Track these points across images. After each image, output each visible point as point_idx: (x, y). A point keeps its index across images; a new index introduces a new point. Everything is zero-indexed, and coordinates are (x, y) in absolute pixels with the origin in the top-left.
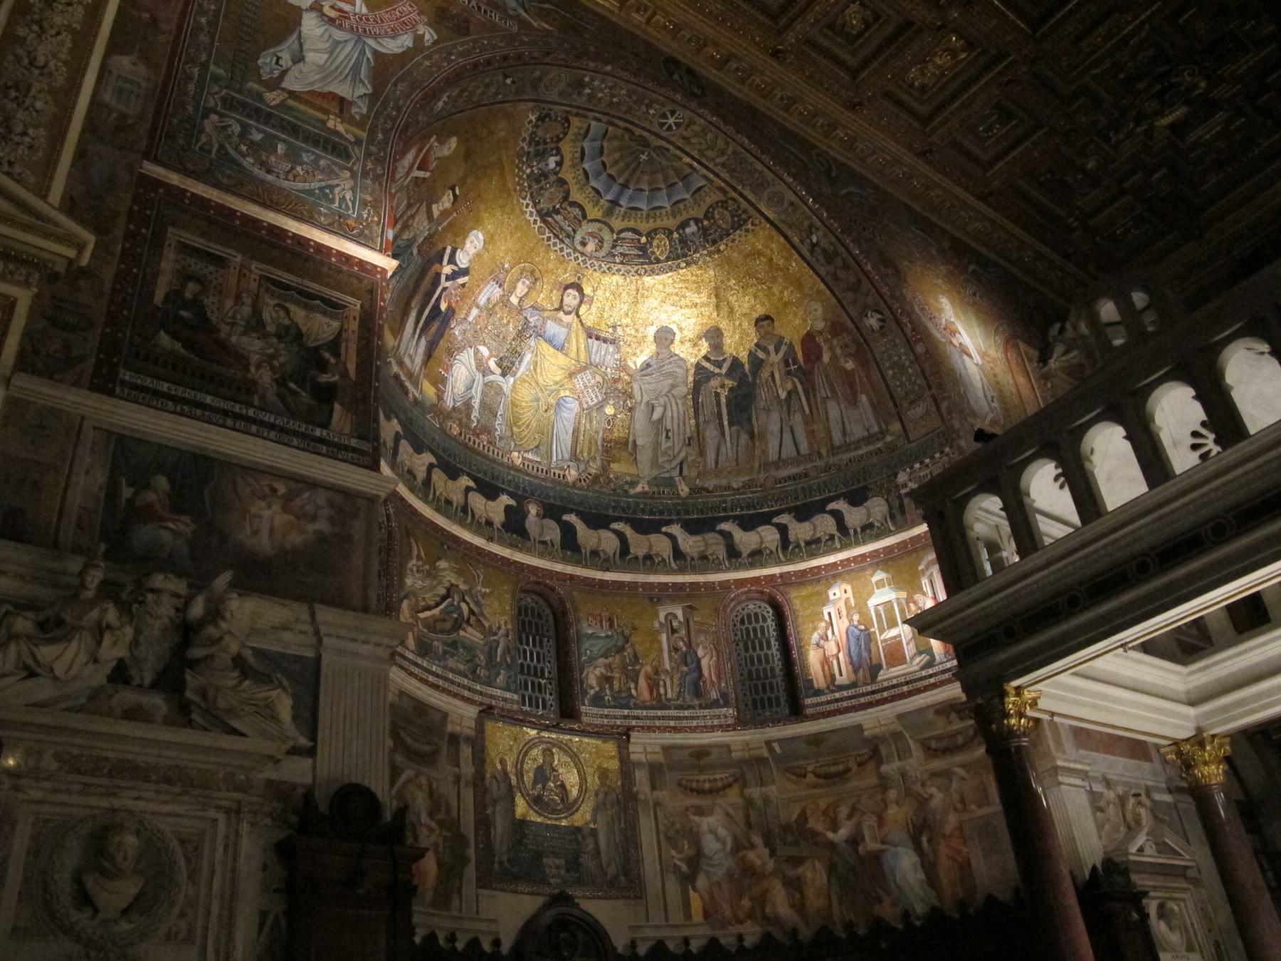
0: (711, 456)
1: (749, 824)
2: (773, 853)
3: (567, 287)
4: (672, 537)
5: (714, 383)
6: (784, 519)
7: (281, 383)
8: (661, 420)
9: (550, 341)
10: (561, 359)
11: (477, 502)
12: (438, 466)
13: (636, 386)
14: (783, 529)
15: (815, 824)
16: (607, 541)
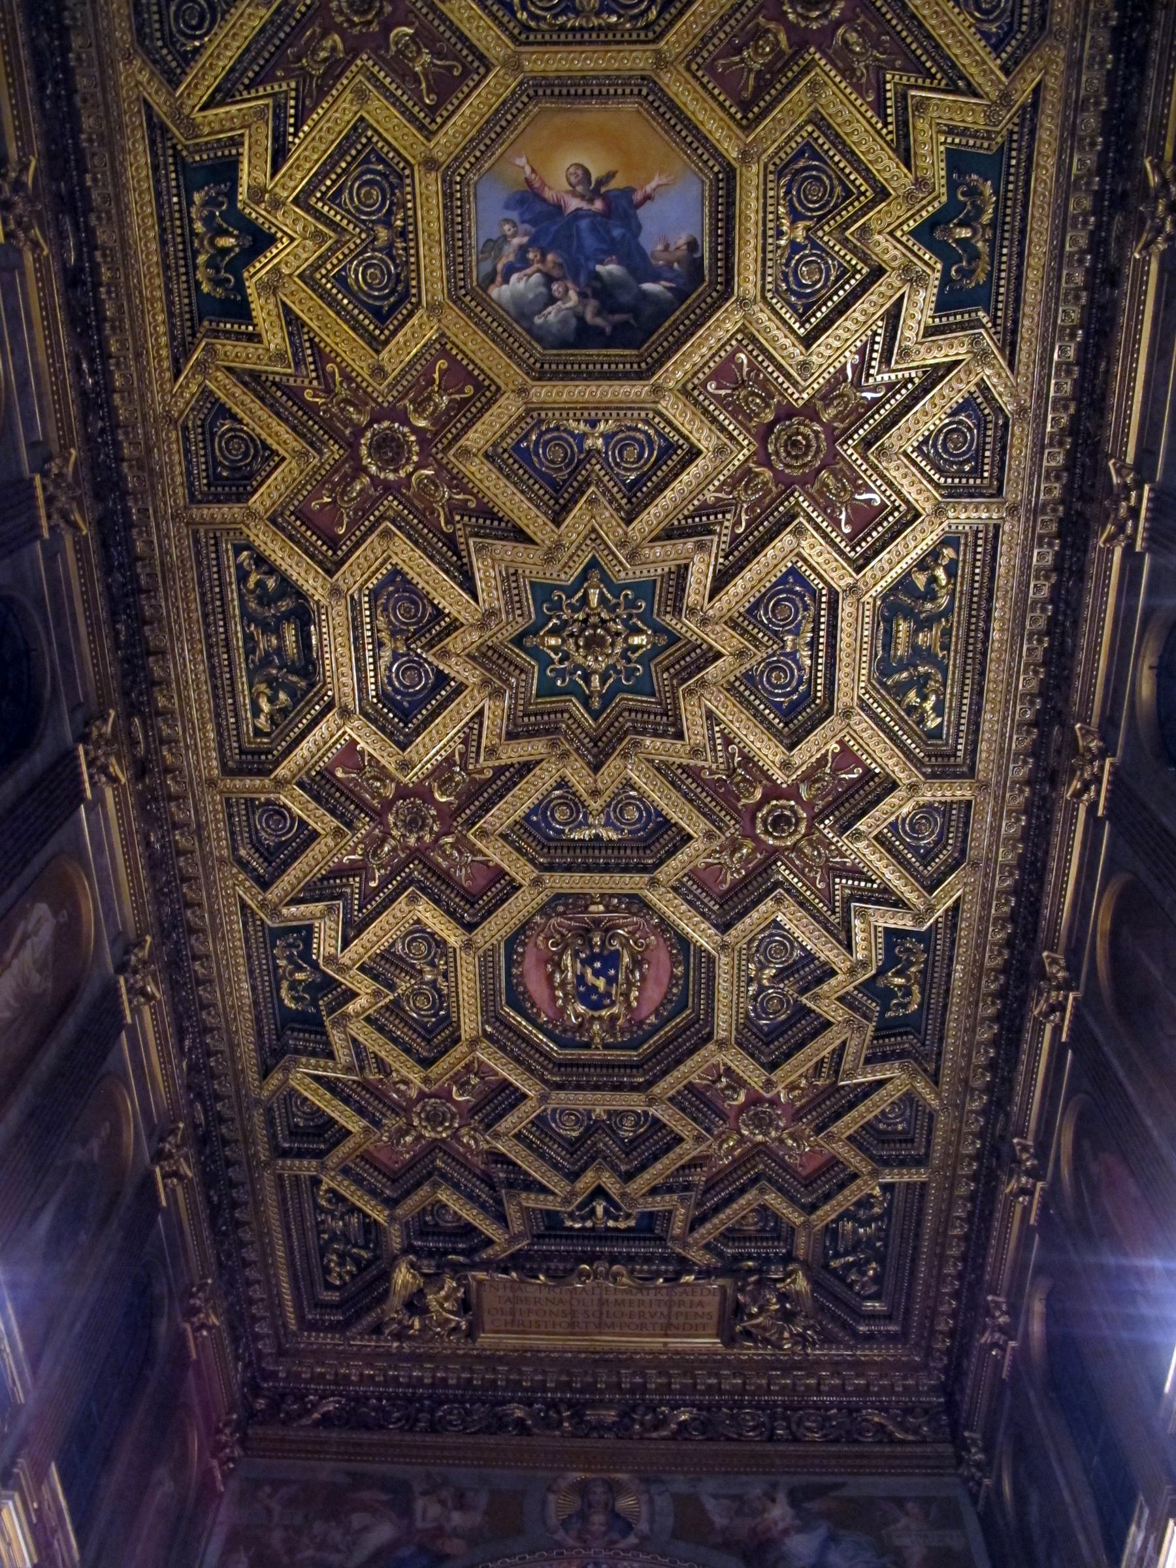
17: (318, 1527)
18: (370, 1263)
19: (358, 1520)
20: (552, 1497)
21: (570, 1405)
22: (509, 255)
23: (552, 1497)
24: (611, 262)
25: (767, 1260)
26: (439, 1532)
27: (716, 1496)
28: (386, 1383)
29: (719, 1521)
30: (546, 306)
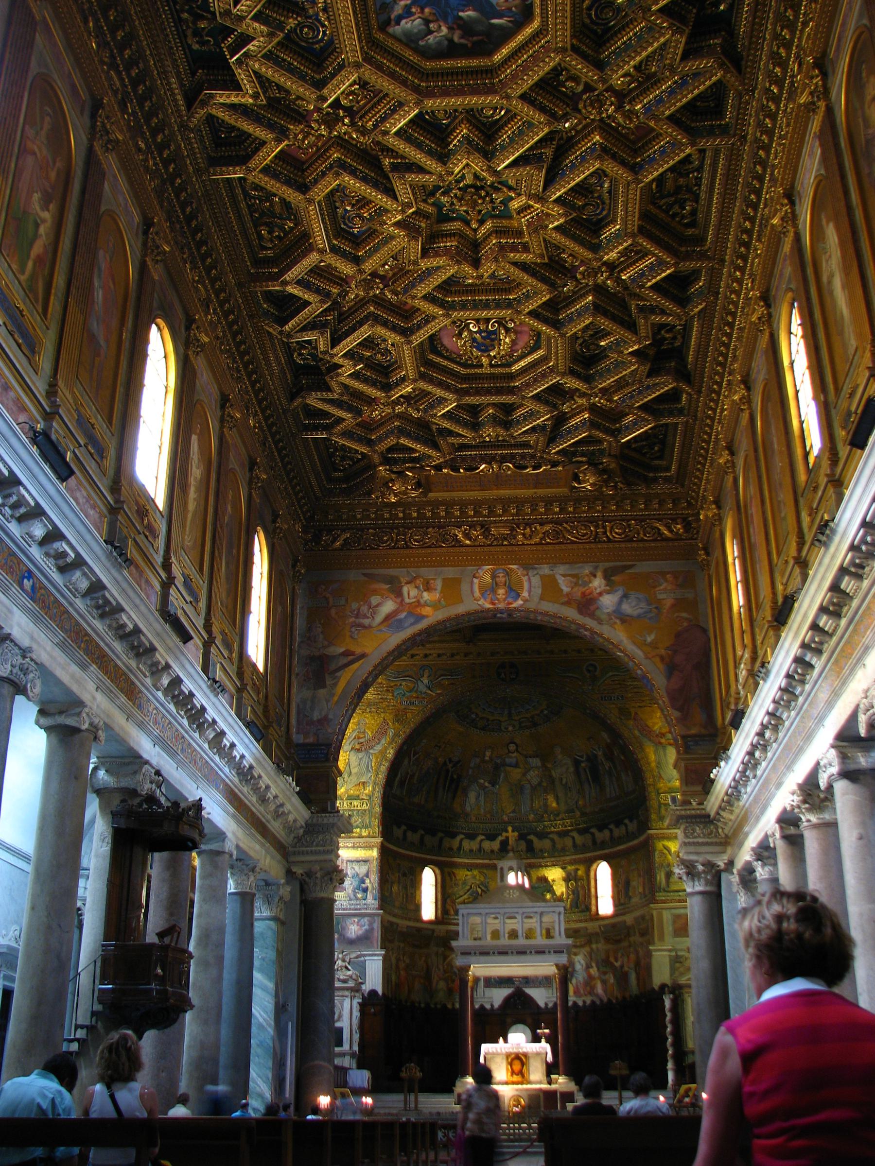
0: (587, 797)
1: (591, 959)
2: (598, 970)
3: (508, 745)
4: (573, 838)
5: (583, 765)
6: (612, 826)
7: (354, 891)
8: (566, 783)
9: (510, 766)
10: (518, 770)
11: (487, 845)
12: (466, 838)
13: (553, 772)
14: (611, 831)
15: (612, 959)
16: (547, 843)
17: (355, 606)
18: (359, 460)
19: (375, 600)
20: (476, 581)
21: (482, 526)
22: (398, 10)
23: (476, 581)
24: (469, 10)
25: (593, 453)
26: (418, 604)
27: (564, 576)
28: (376, 519)
29: (566, 589)
30: (426, 36)
